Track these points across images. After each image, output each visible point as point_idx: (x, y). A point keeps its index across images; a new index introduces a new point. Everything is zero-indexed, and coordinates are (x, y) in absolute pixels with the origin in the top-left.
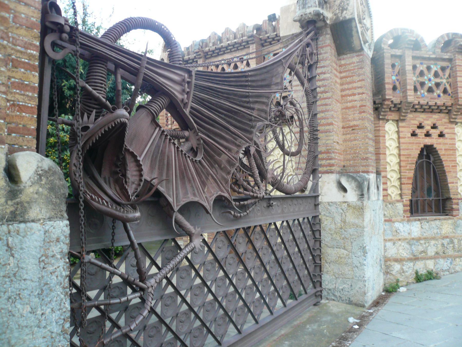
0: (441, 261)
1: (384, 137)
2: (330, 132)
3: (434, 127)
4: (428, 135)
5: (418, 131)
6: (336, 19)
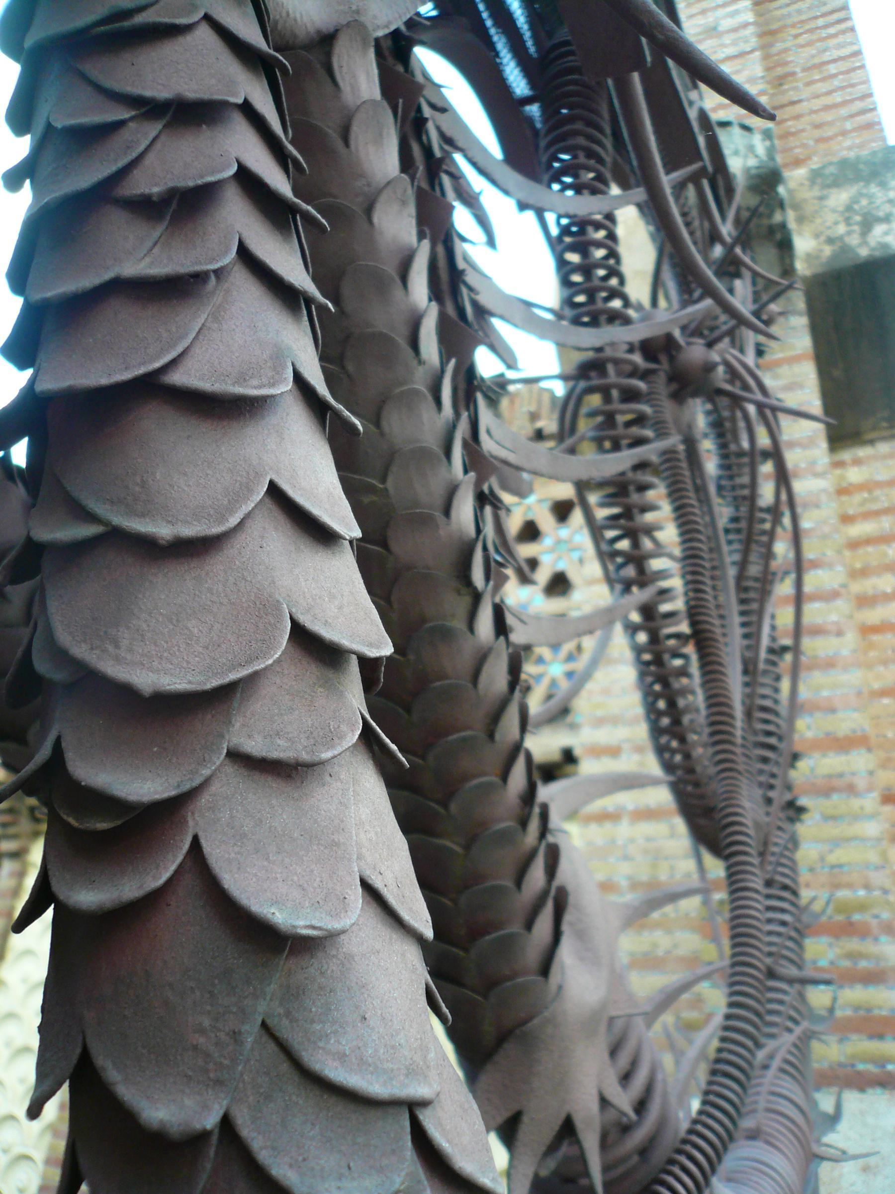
2: (851, 790)
6: (834, 257)
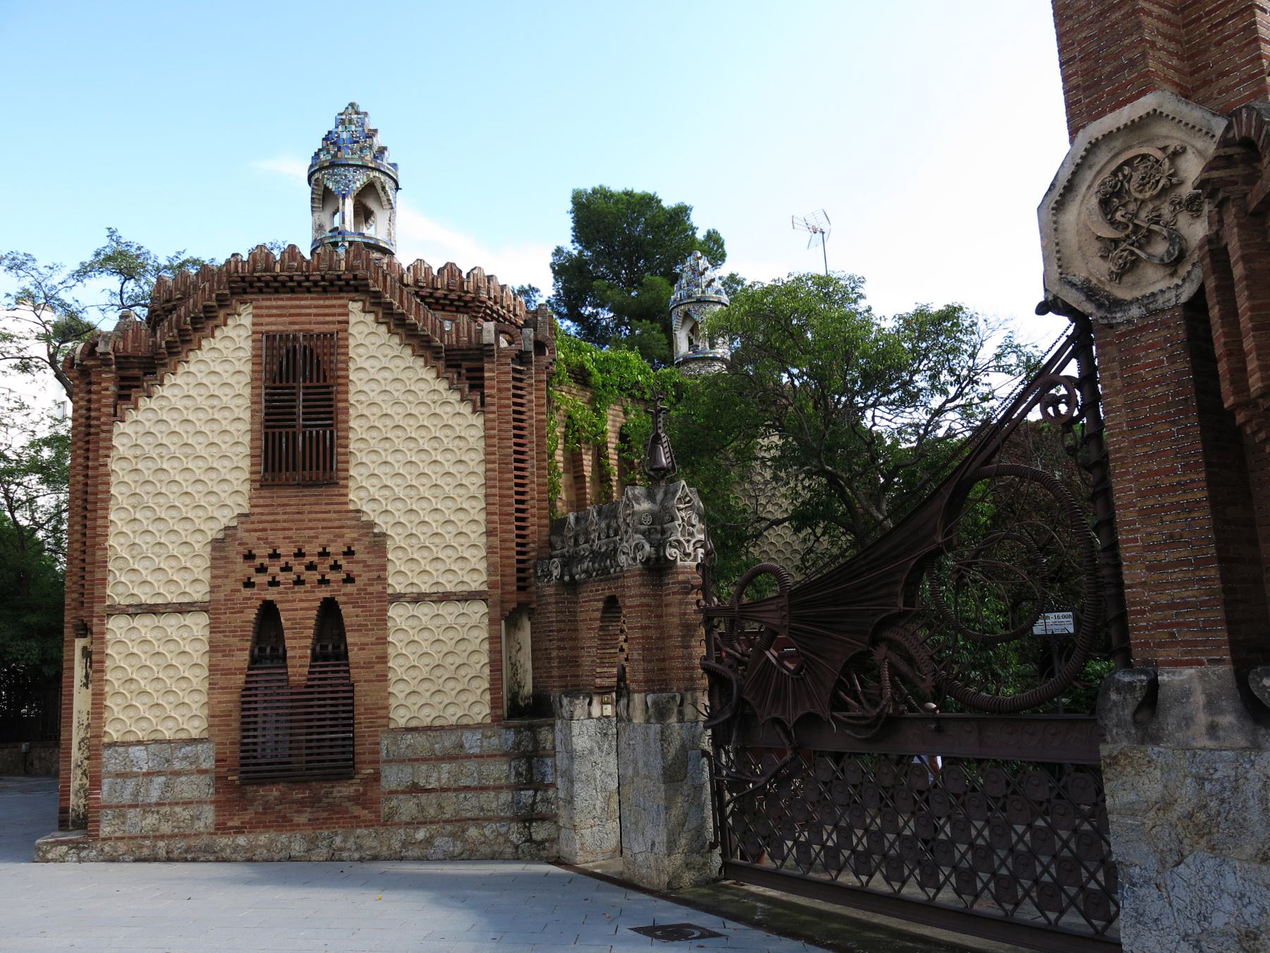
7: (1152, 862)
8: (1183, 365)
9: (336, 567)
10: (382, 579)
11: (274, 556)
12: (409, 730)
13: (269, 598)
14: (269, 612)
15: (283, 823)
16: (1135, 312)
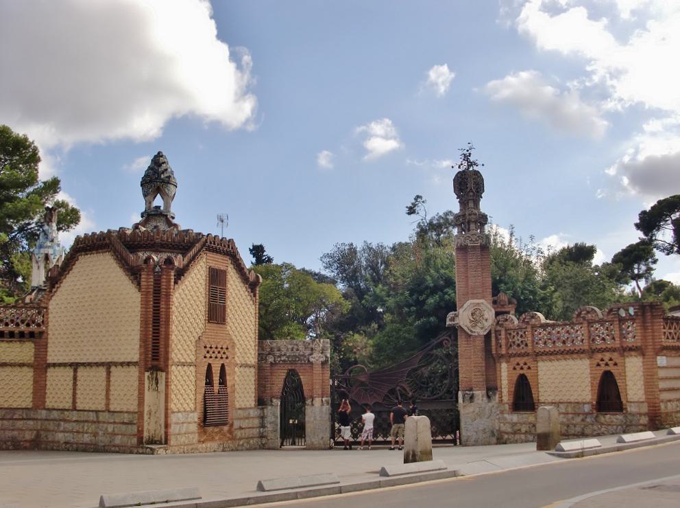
0: (529, 436)
1: (501, 371)
3: (525, 364)
4: (522, 368)
5: (517, 367)
7: (470, 421)
8: (483, 344)
9: (224, 353)
10: (234, 358)
11: (211, 348)
12: (240, 409)
13: (210, 362)
14: (209, 365)
15: (213, 439)
16: (476, 334)
